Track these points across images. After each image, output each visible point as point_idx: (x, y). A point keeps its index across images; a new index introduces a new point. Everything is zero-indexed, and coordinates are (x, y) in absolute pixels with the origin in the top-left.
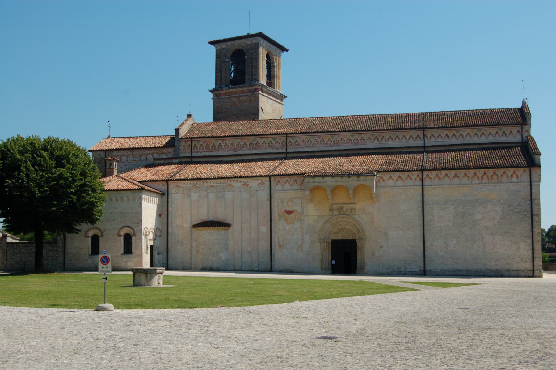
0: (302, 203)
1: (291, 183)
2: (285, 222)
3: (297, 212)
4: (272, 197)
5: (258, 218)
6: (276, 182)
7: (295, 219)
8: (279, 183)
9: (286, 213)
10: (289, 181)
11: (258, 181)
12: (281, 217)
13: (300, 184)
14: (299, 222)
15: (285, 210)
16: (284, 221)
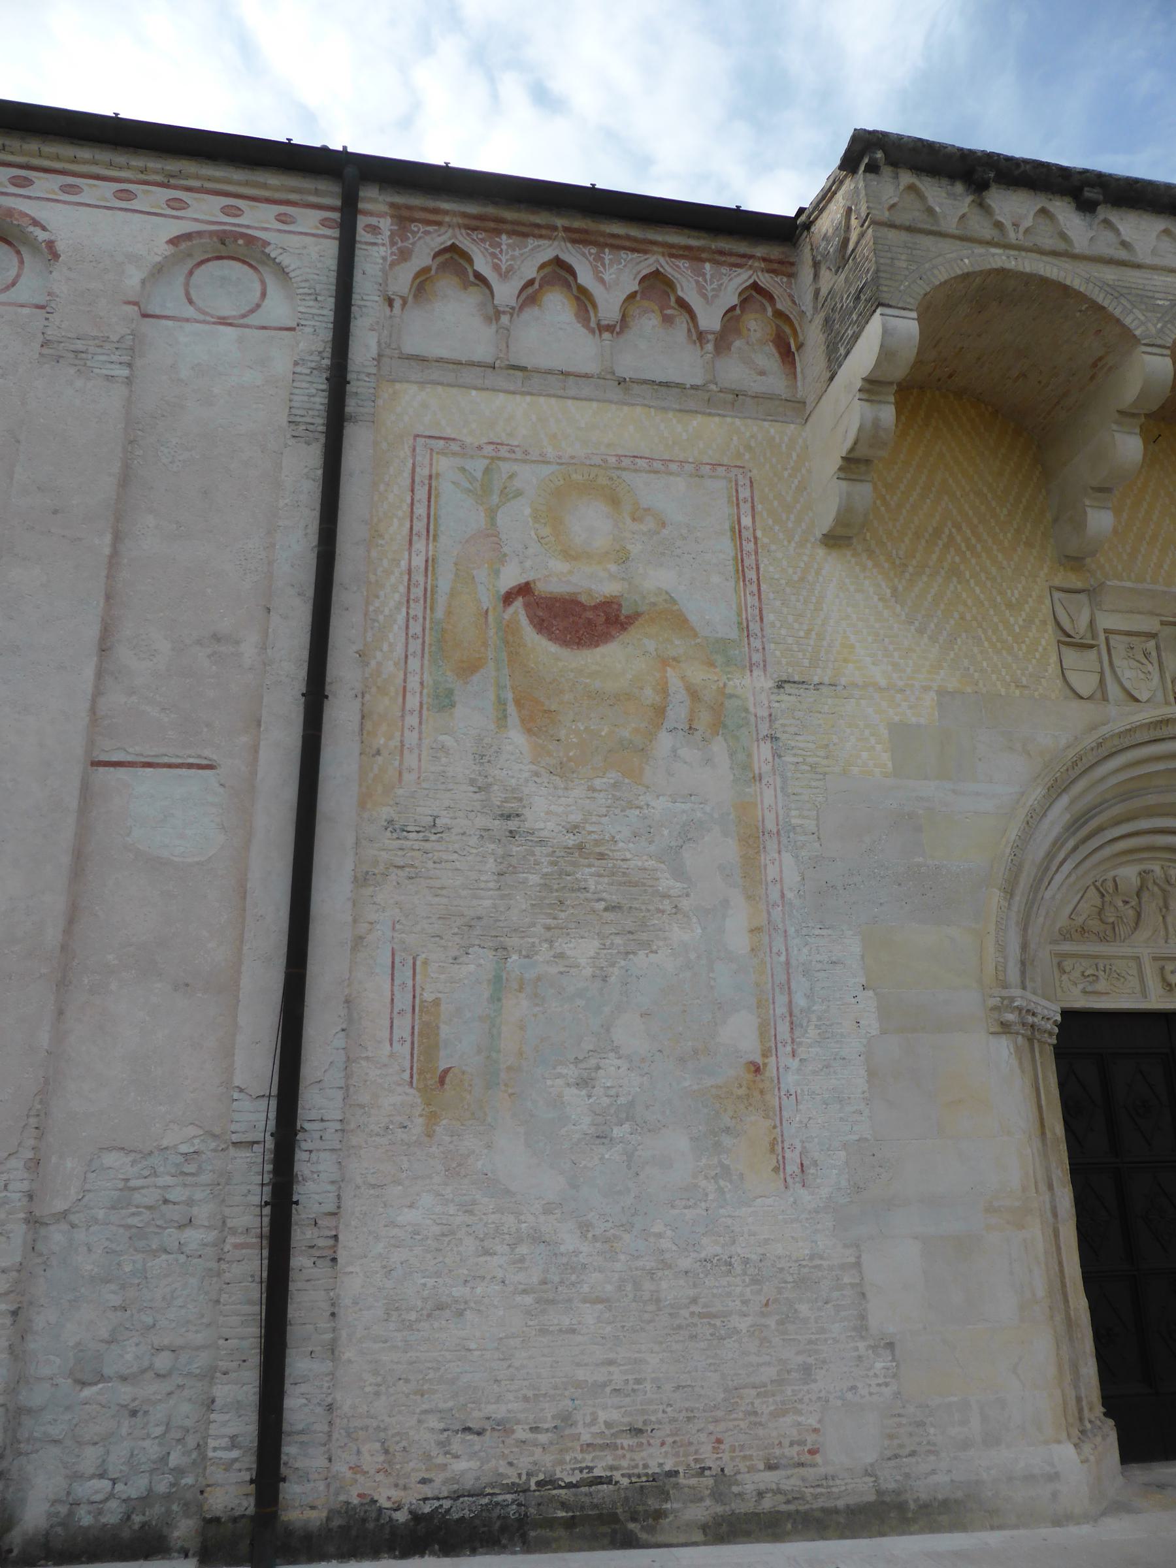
0: (737, 532)
1: (609, 305)
2: (517, 738)
3: (679, 622)
4: (351, 407)
5: (104, 648)
6: (422, 258)
7: (660, 711)
8: (447, 285)
9: (541, 626)
10: (585, 277)
11: (176, 204)
12: (469, 669)
13: (710, 319)
14: (719, 747)
15: (525, 590)
16: (502, 719)
